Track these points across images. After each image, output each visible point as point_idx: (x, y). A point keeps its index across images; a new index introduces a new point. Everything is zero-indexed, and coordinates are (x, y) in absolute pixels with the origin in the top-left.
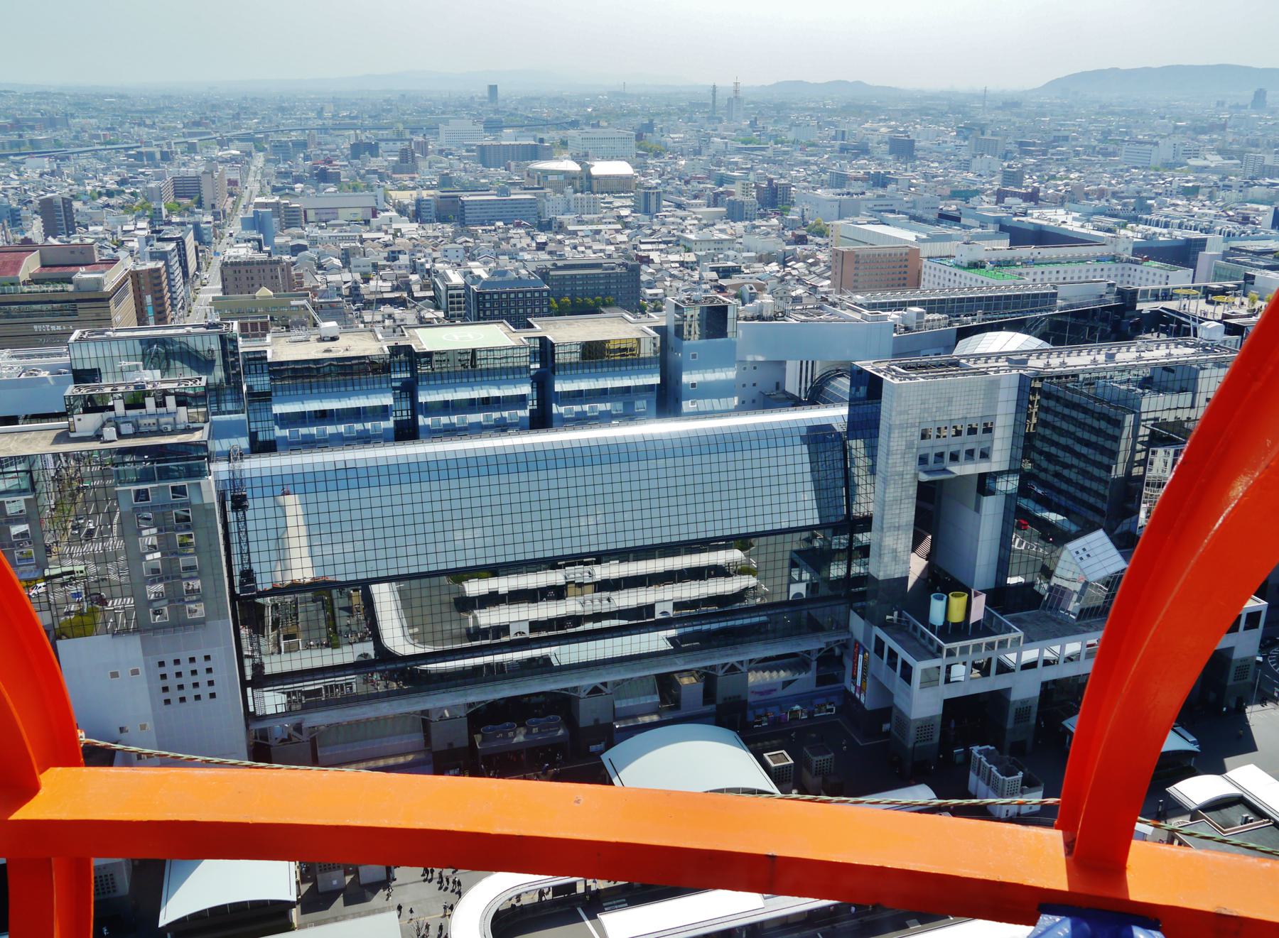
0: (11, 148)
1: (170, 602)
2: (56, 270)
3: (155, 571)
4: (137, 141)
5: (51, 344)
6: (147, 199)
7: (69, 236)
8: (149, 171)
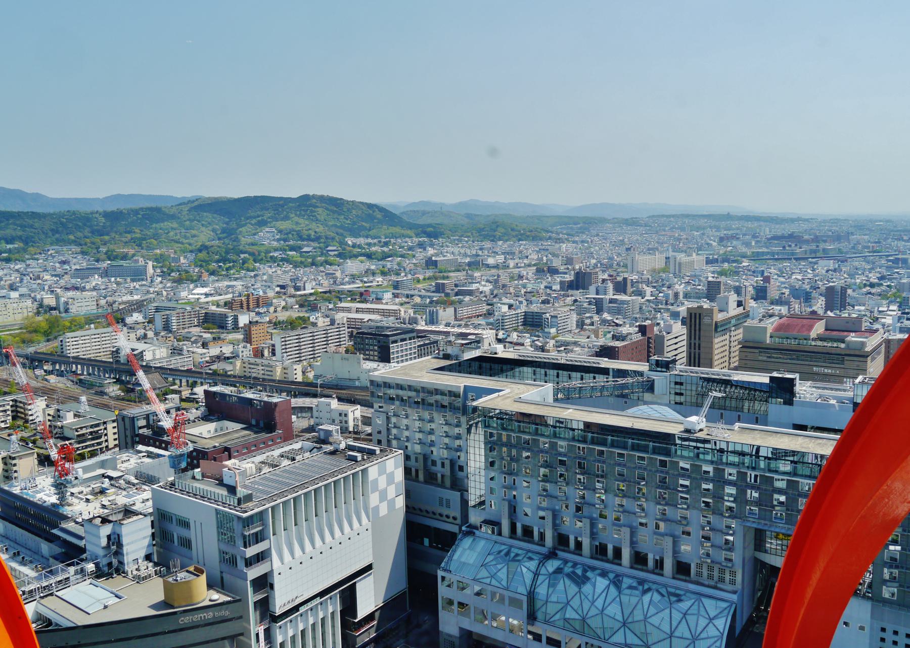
0: (811, 254)
1: (900, 586)
2: (835, 333)
3: (893, 559)
4: (895, 251)
5: (829, 381)
6: (898, 290)
7: (840, 311)
8: (902, 271)
